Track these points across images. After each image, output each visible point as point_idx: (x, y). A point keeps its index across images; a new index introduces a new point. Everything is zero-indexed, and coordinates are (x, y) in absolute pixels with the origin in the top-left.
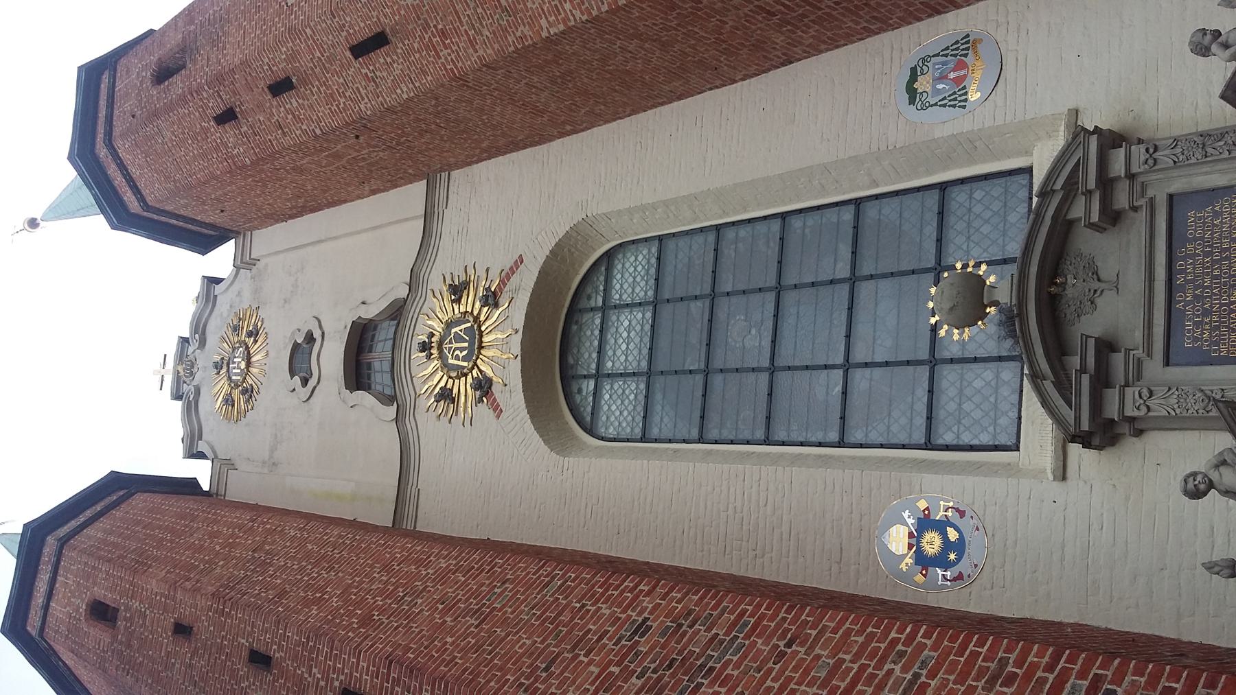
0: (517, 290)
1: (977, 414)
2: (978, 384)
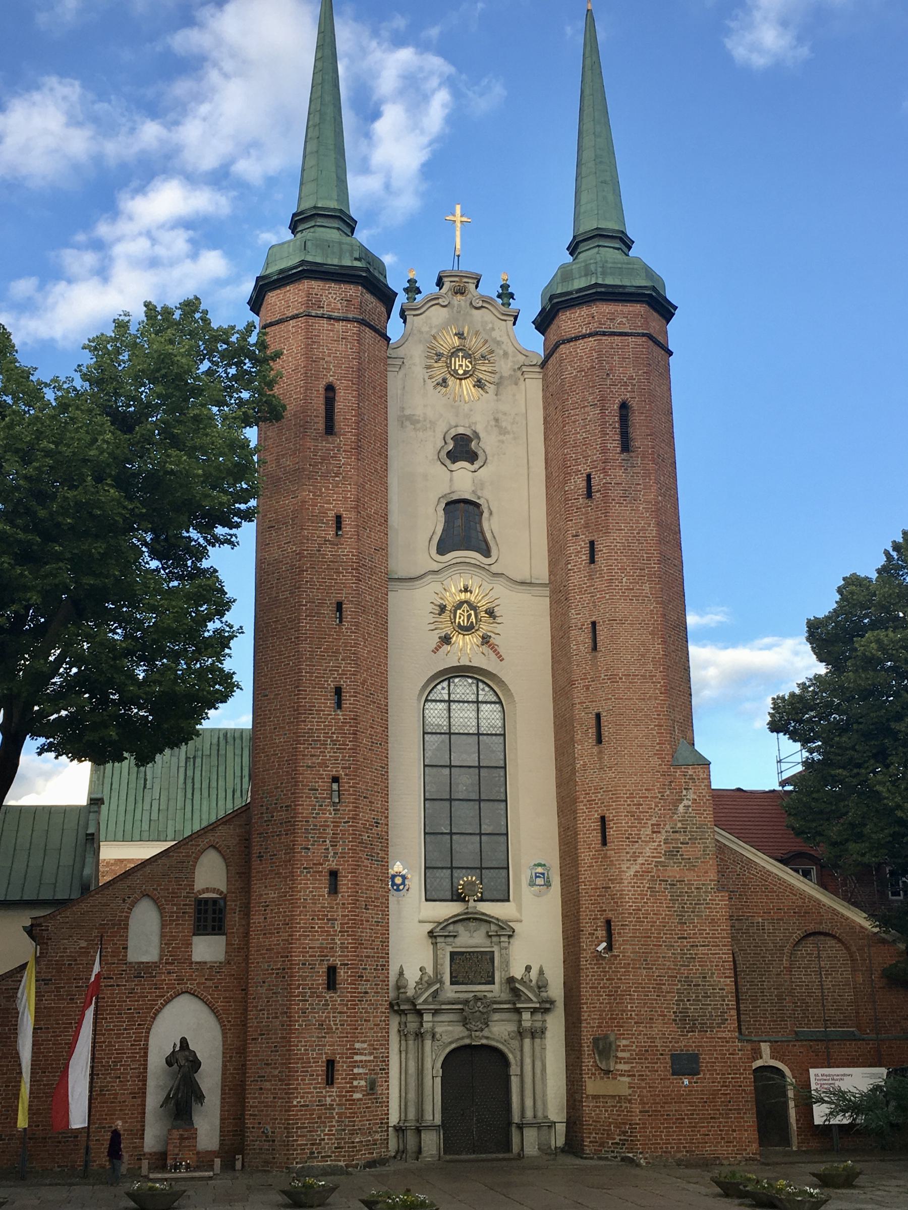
0: (489, 659)
1: (435, 884)
2: (445, 884)
